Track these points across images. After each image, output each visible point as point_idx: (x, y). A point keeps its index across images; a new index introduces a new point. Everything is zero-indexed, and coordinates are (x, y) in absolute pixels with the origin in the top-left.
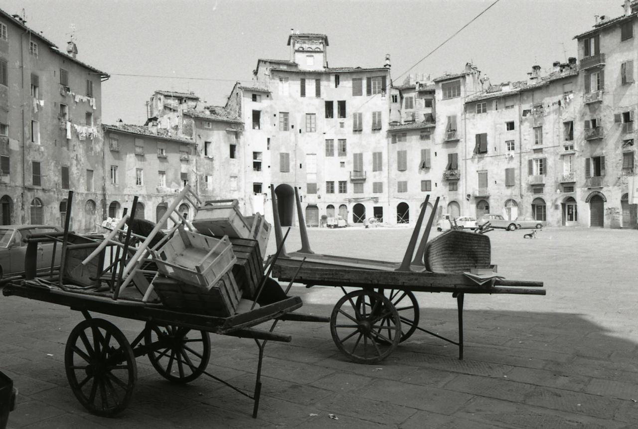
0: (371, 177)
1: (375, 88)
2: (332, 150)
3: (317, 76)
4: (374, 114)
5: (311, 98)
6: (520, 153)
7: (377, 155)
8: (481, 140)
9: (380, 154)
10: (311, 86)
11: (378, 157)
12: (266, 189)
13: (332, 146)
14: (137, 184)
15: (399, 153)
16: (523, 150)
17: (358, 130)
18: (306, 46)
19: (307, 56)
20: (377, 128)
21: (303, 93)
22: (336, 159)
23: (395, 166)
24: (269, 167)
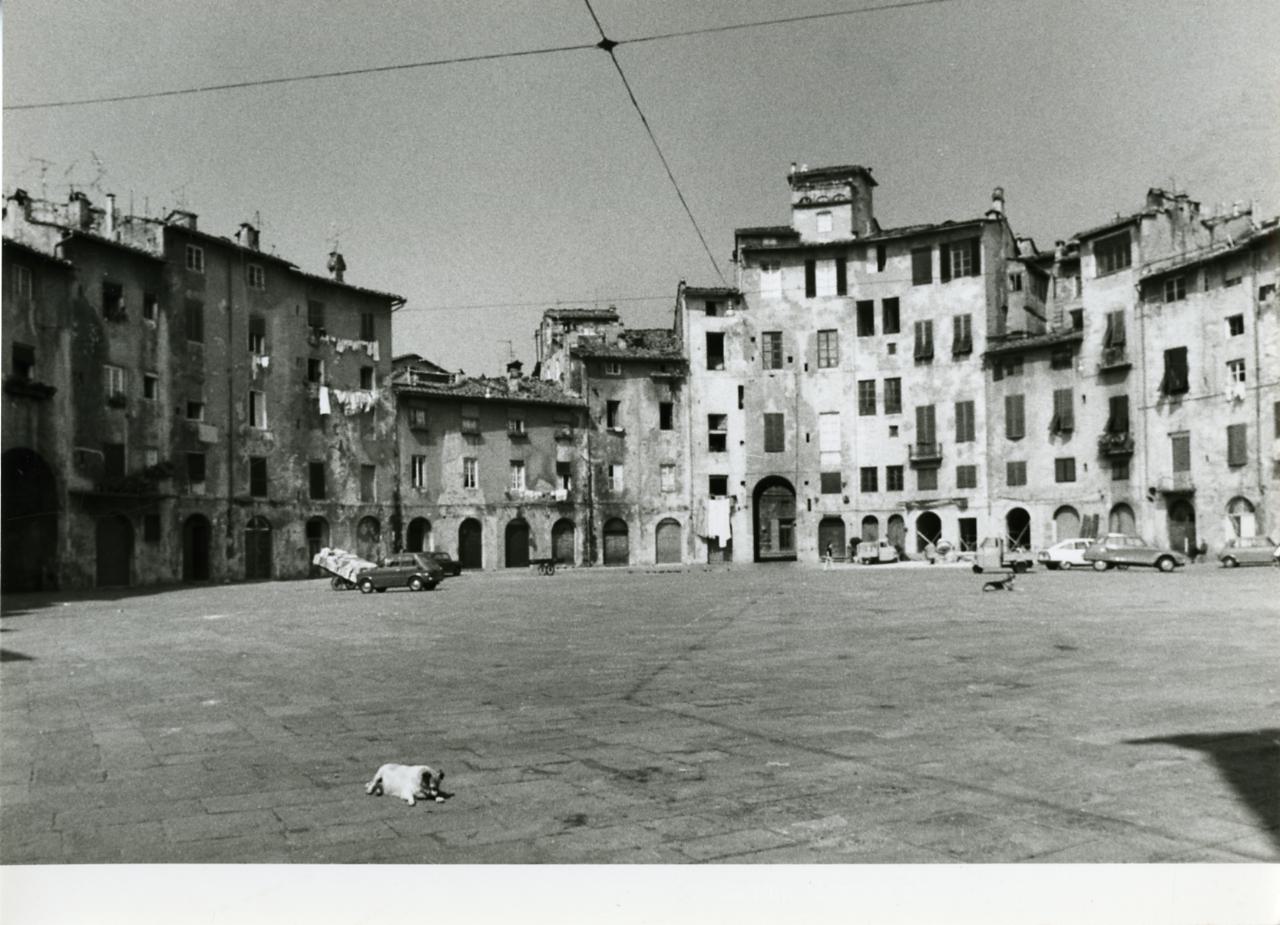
0: (953, 454)
1: (957, 265)
2: (872, 404)
3: (840, 253)
4: (957, 320)
5: (827, 299)
6: (1258, 388)
7: (964, 407)
8: (1176, 360)
9: (970, 405)
10: (826, 274)
11: (965, 413)
12: (734, 487)
13: (872, 393)
14: (466, 484)
15: (1008, 400)
16: (1264, 381)
17: (924, 355)
18: (815, 194)
19: (818, 214)
20: (962, 348)
21: (811, 291)
22: (881, 419)
23: (1001, 428)
24: (742, 443)
